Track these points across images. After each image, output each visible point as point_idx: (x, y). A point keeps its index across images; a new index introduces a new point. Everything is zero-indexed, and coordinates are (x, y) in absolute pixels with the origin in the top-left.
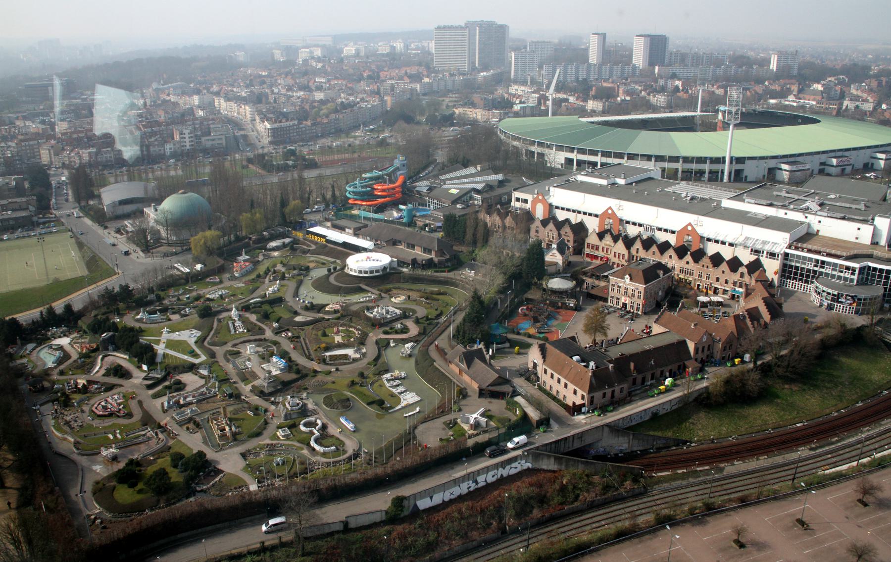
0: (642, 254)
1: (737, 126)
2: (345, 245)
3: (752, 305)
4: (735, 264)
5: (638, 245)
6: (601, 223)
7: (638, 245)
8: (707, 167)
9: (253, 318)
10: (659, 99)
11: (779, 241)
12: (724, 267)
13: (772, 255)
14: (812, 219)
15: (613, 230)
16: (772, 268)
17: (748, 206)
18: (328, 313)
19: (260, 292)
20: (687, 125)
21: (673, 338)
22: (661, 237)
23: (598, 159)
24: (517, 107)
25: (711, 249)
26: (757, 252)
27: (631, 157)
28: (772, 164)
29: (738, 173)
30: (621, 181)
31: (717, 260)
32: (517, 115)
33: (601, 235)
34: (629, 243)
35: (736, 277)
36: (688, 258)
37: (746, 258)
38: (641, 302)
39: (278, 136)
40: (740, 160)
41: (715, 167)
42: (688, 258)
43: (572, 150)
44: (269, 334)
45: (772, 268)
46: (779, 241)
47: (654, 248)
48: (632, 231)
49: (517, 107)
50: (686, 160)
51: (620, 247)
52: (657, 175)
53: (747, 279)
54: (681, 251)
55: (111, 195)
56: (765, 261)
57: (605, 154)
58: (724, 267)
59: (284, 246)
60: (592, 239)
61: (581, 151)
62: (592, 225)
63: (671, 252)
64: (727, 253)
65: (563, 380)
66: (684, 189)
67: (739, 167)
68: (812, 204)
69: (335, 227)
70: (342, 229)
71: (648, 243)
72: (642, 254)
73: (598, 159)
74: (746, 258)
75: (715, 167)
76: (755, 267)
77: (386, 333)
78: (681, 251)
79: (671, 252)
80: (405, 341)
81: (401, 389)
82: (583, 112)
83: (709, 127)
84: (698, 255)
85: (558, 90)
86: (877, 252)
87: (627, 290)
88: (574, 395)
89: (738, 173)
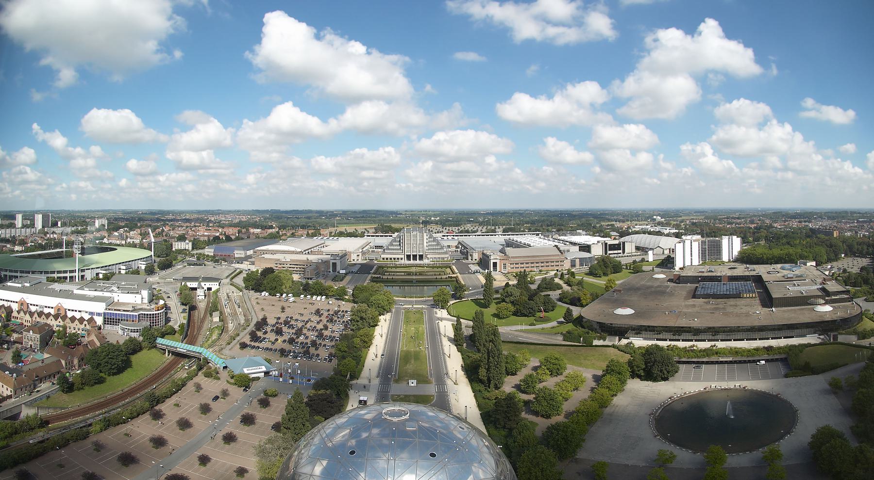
0: (38, 319)
3: (90, 339)
4: (81, 320)
7: (36, 315)
8: (68, 275)
11: (101, 307)
12: (77, 322)
13: (99, 314)
14: (115, 295)
15: (24, 307)
16: (99, 321)
17: (86, 292)
21: (55, 359)
22: (46, 311)
23: (19, 274)
25: (70, 314)
26: (92, 313)
27: (33, 272)
29: (83, 277)
30: (27, 285)
33: (18, 312)
34: (31, 314)
35: (83, 326)
36: (60, 320)
37: (87, 317)
38: (38, 343)
41: (72, 275)
42: (60, 320)
43: (6, 271)
45: (99, 321)
46: (101, 307)
47: (43, 316)
48: (33, 309)
51: (28, 317)
53: (88, 327)
54: (56, 317)
56: (96, 318)
57: (22, 272)
58: (77, 322)
60: (15, 314)
61: (11, 271)
62: (15, 307)
63: (51, 317)
64: (78, 315)
66: (57, 286)
68: (115, 289)
71: (40, 314)
72: (38, 319)
73: (19, 274)
74: (87, 317)
75: (72, 275)
76: (91, 320)
78: (56, 317)
79: (51, 317)
84: (64, 317)
86: (145, 306)
87: (32, 338)
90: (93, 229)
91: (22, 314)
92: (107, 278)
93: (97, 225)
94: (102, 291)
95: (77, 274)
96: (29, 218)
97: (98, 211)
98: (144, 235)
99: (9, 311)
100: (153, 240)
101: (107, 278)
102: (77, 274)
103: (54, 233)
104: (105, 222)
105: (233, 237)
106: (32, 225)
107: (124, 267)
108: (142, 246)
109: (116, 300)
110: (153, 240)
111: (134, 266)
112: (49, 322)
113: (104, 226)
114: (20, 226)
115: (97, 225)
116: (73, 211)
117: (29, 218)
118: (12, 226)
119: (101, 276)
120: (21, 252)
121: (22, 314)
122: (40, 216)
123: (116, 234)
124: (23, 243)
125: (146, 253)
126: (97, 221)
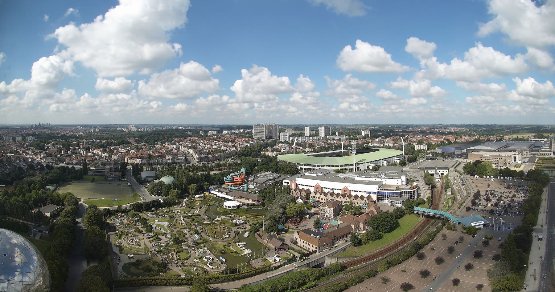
1: (355, 154)
2: (223, 198)
3: (370, 210)
4: (362, 197)
8: (348, 167)
9: (189, 220)
11: (374, 188)
12: (359, 199)
13: (374, 193)
16: (374, 197)
17: (363, 179)
18: (217, 221)
19: (191, 212)
20: (339, 155)
24: (282, 151)
25: (353, 194)
26: (368, 193)
29: (358, 168)
32: (282, 154)
35: (363, 201)
37: (366, 195)
38: (332, 214)
39: (201, 160)
40: (358, 164)
41: (350, 167)
42: (347, 197)
44: (193, 227)
45: (374, 197)
47: (335, 196)
49: (282, 151)
50: (341, 166)
53: (367, 202)
54: (344, 196)
55: (144, 175)
56: (371, 195)
58: (359, 199)
59: (201, 197)
63: (341, 196)
64: (359, 194)
65: (308, 243)
67: (358, 166)
68: (384, 176)
69: (219, 191)
70: (222, 192)
74: (366, 195)
75: (350, 167)
76: (369, 198)
77: (238, 228)
79: (341, 196)
80: (246, 231)
81: (244, 248)
82: (305, 152)
83: (347, 154)
84: (350, 196)
85: (296, 145)
88: (311, 248)
90: (361, 137)
92: (376, 169)
93: (363, 134)
94: (374, 177)
95: (354, 167)
96: (315, 130)
97: (362, 125)
98: (395, 141)
99: (308, 193)
100: (403, 144)
101: (376, 169)
102: (354, 167)
103: (333, 139)
104: (369, 133)
105: (452, 142)
106: (318, 134)
107: (386, 162)
108: (395, 148)
109: (384, 184)
110: (403, 144)
111: (392, 161)
112: (339, 199)
113: (368, 135)
114: (308, 134)
115: (363, 134)
116: (345, 125)
117: (315, 130)
118: (302, 135)
120: (311, 152)
122: (323, 128)
123: (377, 140)
124: (311, 146)
125: (399, 152)
126: (363, 132)
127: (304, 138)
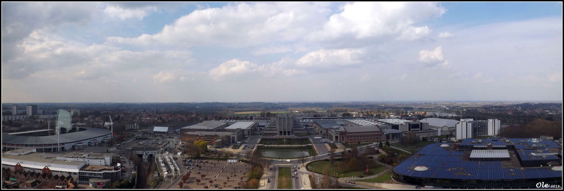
5: (29, 175)
6: (15, 169)
7: (29, 175)
10: (37, 126)
12: (59, 179)
13: (75, 173)
20: (46, 134)
22: (37, 171)
23: (15, 147)
25: (54, 174)
26: (70, 173)
28: (73, 144)
29: (63, 148)
31: (57, 177)
33: (16, 173)
34: (26, 174)
40: (63, 144)
47: (34, 176)
48: (27, 170)
50: (45, 145)
52: (35, 150)
56: (72, 175)
58: (59, 179)
60: (13, 174)
61: (9, 144)
62: (13, 169)
64: (60, 175)
75: (54, 147)
78: (44, 176)
89: (63, 148)
91: (18, 174)
114: (15, 113)
119: (76, 148)
121: (18, 174)
122: (31, 107)
127: (10, 117)
